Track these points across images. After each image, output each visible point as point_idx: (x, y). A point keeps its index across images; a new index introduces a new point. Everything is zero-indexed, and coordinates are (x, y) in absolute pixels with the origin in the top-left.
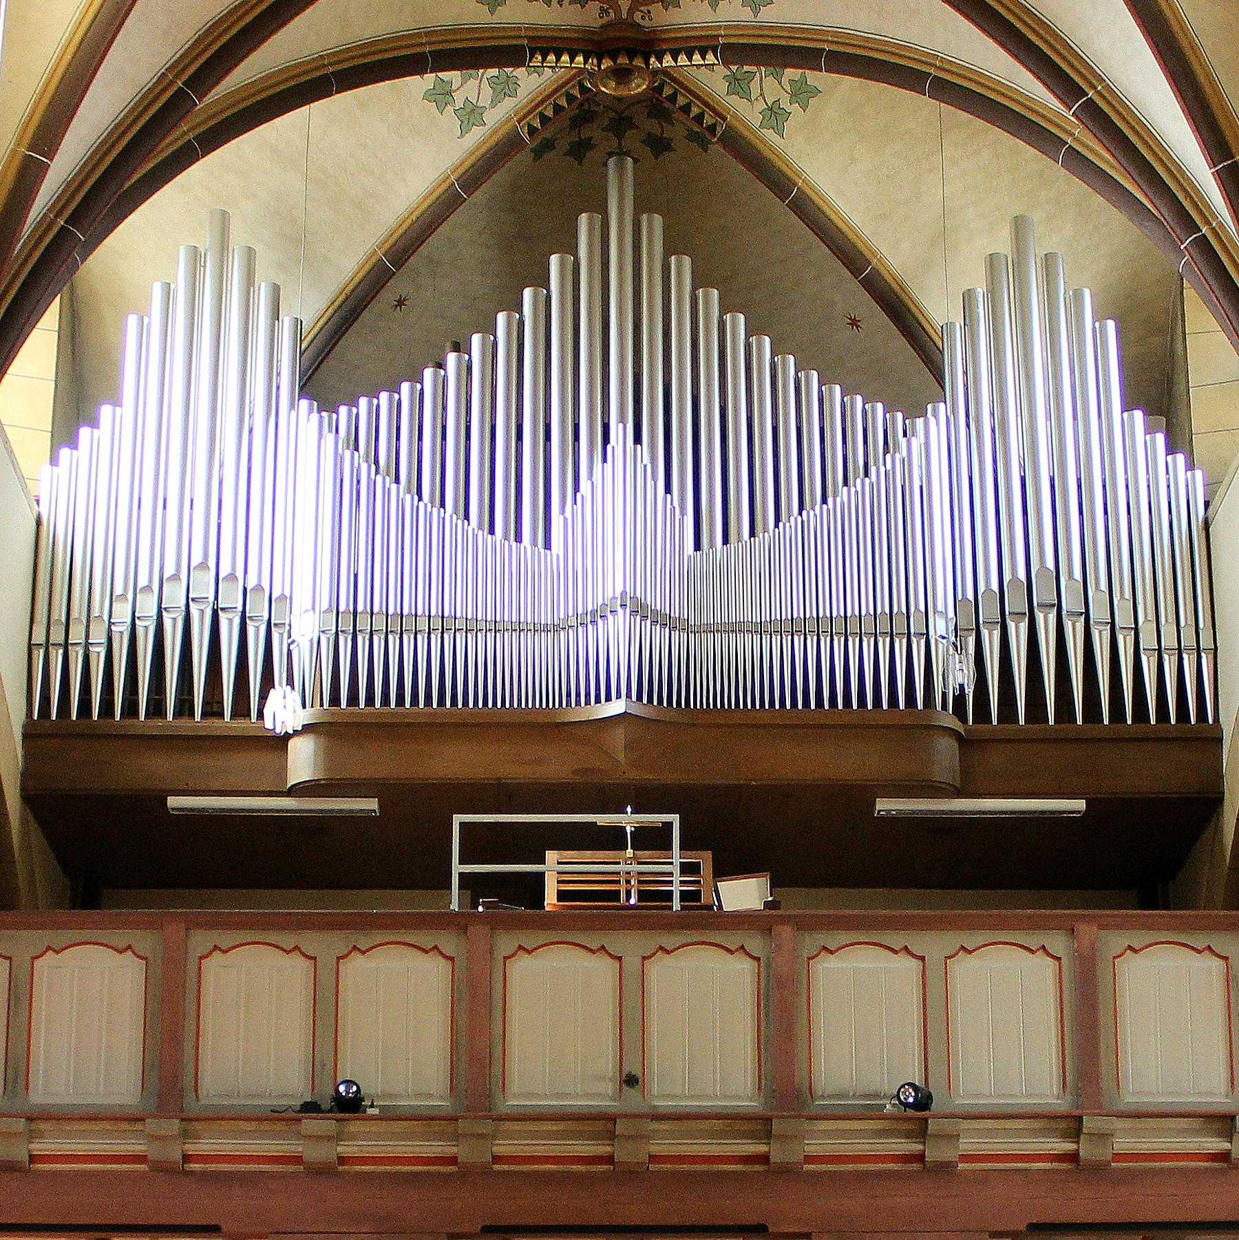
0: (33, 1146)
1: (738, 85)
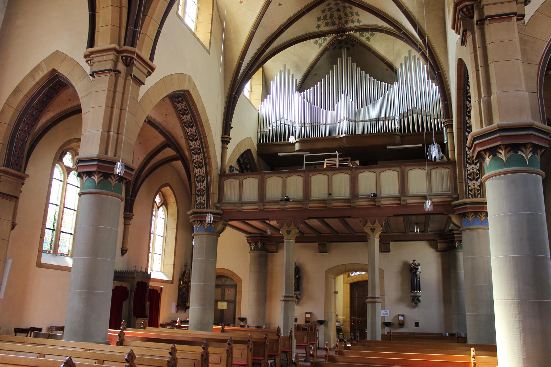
0: (242, 208)
1: (361, 35)
